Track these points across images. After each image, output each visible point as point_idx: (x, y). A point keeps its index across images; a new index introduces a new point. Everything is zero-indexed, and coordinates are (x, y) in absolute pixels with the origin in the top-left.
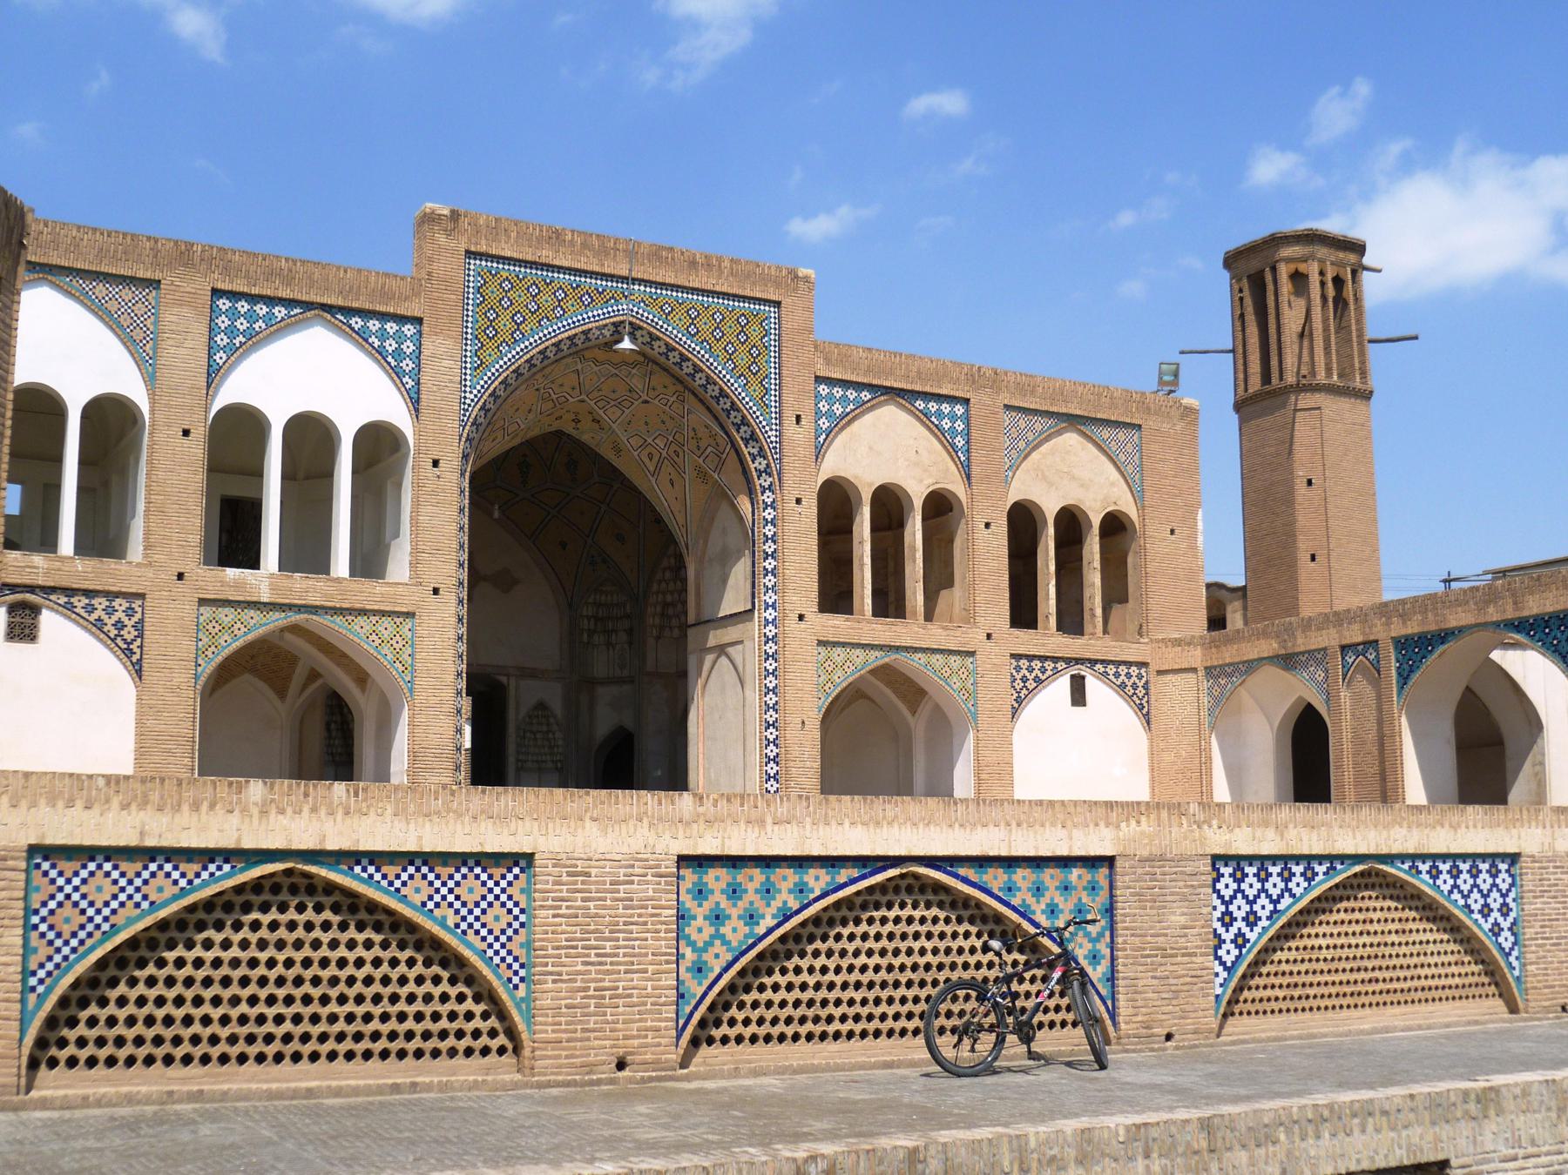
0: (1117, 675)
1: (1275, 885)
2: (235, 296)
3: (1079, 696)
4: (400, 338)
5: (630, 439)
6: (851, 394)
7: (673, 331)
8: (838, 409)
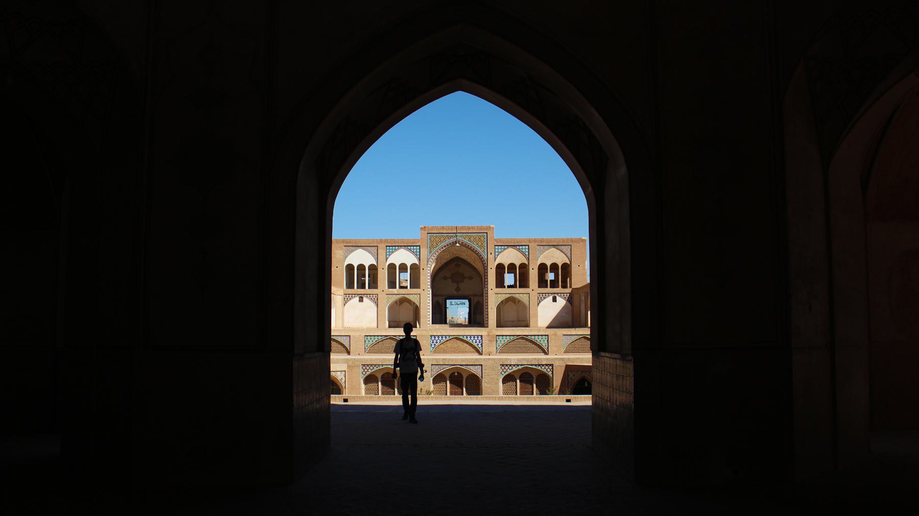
3: (554, 300)
7: (466, 241)
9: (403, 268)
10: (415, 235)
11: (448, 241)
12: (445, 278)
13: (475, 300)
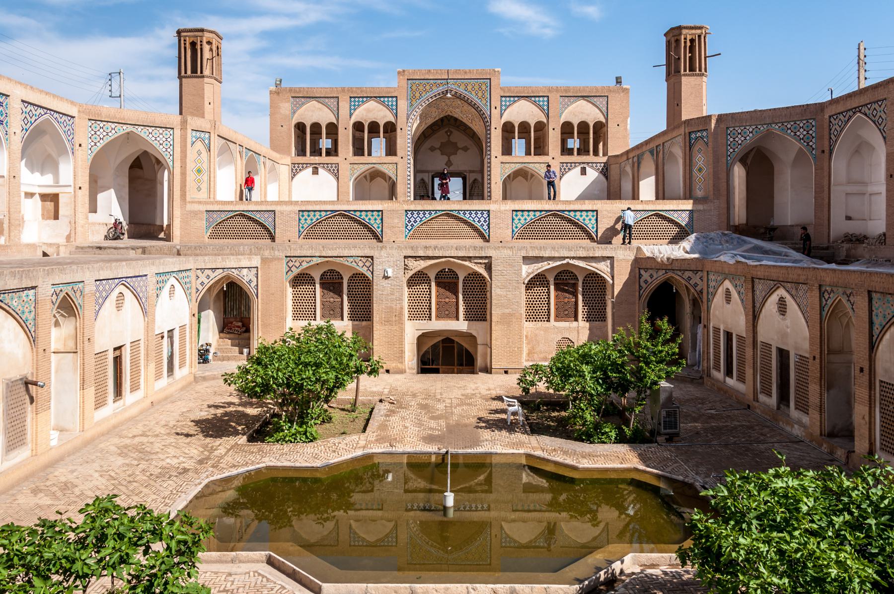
1: (421, 215)
3: (583, 172)
6: (512, 99)
7: (461, 90)
8: (508, 104)
9: (374, 128)
10: (389, 81)
11: (436, 90)
12: (432, 149)
13: (471, 178)
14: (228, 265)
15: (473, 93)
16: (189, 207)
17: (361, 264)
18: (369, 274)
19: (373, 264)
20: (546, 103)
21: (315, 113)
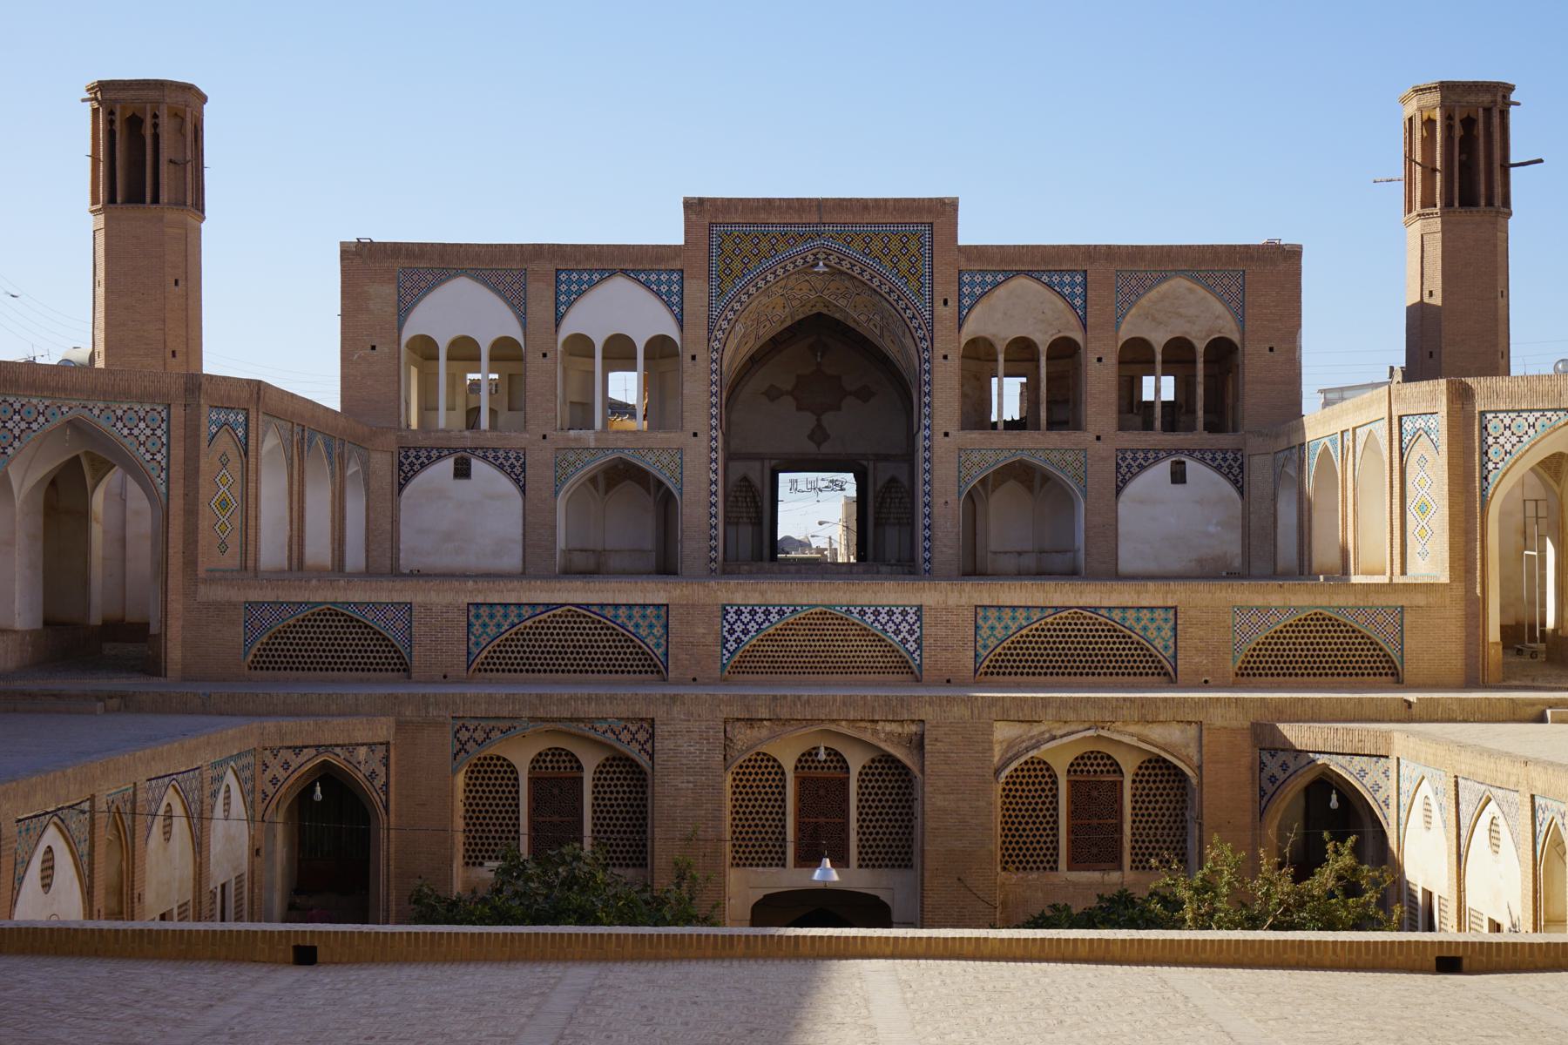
0: (1214, 459)
2: (569, 271)
3: (1178, 476)
4: (669, 283)
5: (859, 315)
8: (978, 291)
9: (620, 353)
12: (773, 394)
14: (327, 738)
15: (886, 261)
16: (207, 593)
17: (625, 736)
18: (643, 760)
19: (652, 736)
20: (1078, 290)
21: (462, 312)
